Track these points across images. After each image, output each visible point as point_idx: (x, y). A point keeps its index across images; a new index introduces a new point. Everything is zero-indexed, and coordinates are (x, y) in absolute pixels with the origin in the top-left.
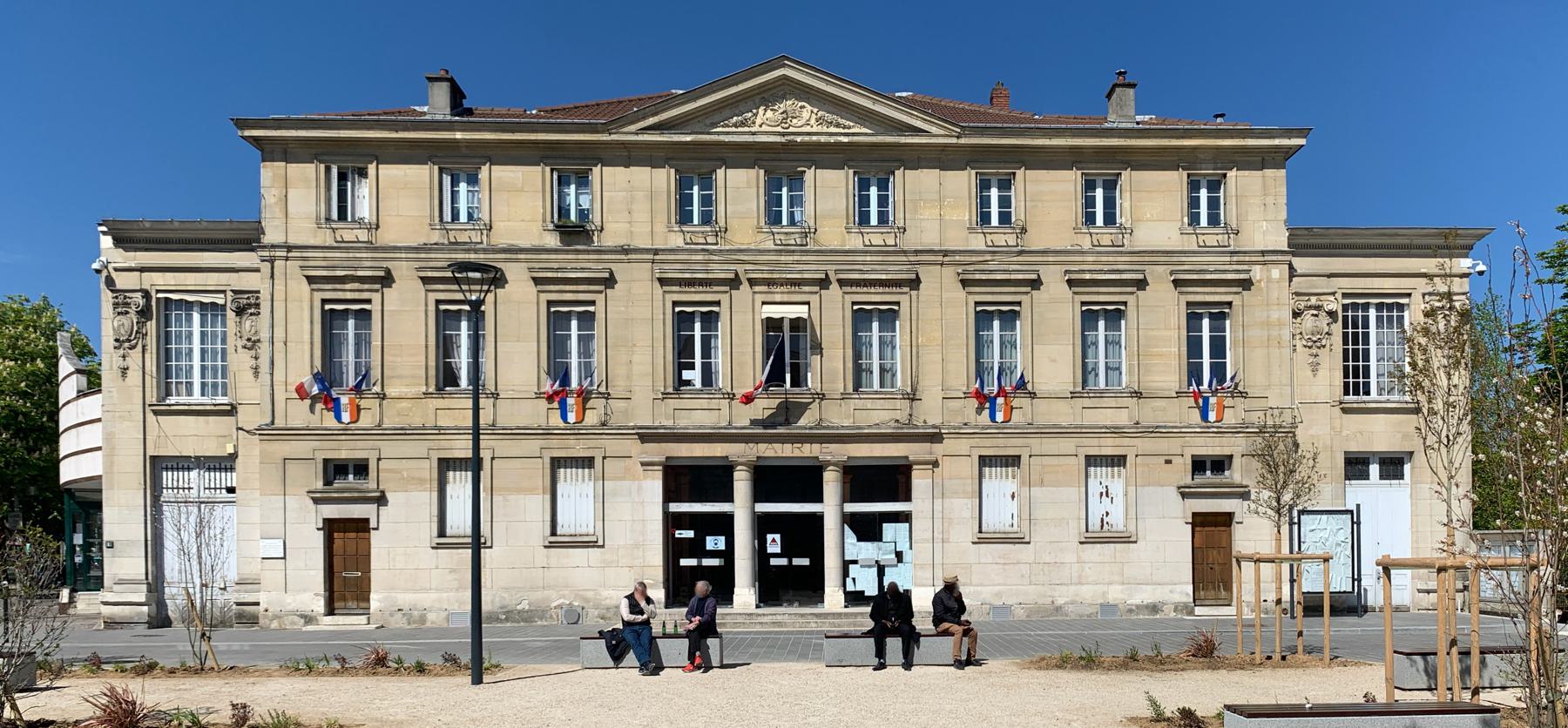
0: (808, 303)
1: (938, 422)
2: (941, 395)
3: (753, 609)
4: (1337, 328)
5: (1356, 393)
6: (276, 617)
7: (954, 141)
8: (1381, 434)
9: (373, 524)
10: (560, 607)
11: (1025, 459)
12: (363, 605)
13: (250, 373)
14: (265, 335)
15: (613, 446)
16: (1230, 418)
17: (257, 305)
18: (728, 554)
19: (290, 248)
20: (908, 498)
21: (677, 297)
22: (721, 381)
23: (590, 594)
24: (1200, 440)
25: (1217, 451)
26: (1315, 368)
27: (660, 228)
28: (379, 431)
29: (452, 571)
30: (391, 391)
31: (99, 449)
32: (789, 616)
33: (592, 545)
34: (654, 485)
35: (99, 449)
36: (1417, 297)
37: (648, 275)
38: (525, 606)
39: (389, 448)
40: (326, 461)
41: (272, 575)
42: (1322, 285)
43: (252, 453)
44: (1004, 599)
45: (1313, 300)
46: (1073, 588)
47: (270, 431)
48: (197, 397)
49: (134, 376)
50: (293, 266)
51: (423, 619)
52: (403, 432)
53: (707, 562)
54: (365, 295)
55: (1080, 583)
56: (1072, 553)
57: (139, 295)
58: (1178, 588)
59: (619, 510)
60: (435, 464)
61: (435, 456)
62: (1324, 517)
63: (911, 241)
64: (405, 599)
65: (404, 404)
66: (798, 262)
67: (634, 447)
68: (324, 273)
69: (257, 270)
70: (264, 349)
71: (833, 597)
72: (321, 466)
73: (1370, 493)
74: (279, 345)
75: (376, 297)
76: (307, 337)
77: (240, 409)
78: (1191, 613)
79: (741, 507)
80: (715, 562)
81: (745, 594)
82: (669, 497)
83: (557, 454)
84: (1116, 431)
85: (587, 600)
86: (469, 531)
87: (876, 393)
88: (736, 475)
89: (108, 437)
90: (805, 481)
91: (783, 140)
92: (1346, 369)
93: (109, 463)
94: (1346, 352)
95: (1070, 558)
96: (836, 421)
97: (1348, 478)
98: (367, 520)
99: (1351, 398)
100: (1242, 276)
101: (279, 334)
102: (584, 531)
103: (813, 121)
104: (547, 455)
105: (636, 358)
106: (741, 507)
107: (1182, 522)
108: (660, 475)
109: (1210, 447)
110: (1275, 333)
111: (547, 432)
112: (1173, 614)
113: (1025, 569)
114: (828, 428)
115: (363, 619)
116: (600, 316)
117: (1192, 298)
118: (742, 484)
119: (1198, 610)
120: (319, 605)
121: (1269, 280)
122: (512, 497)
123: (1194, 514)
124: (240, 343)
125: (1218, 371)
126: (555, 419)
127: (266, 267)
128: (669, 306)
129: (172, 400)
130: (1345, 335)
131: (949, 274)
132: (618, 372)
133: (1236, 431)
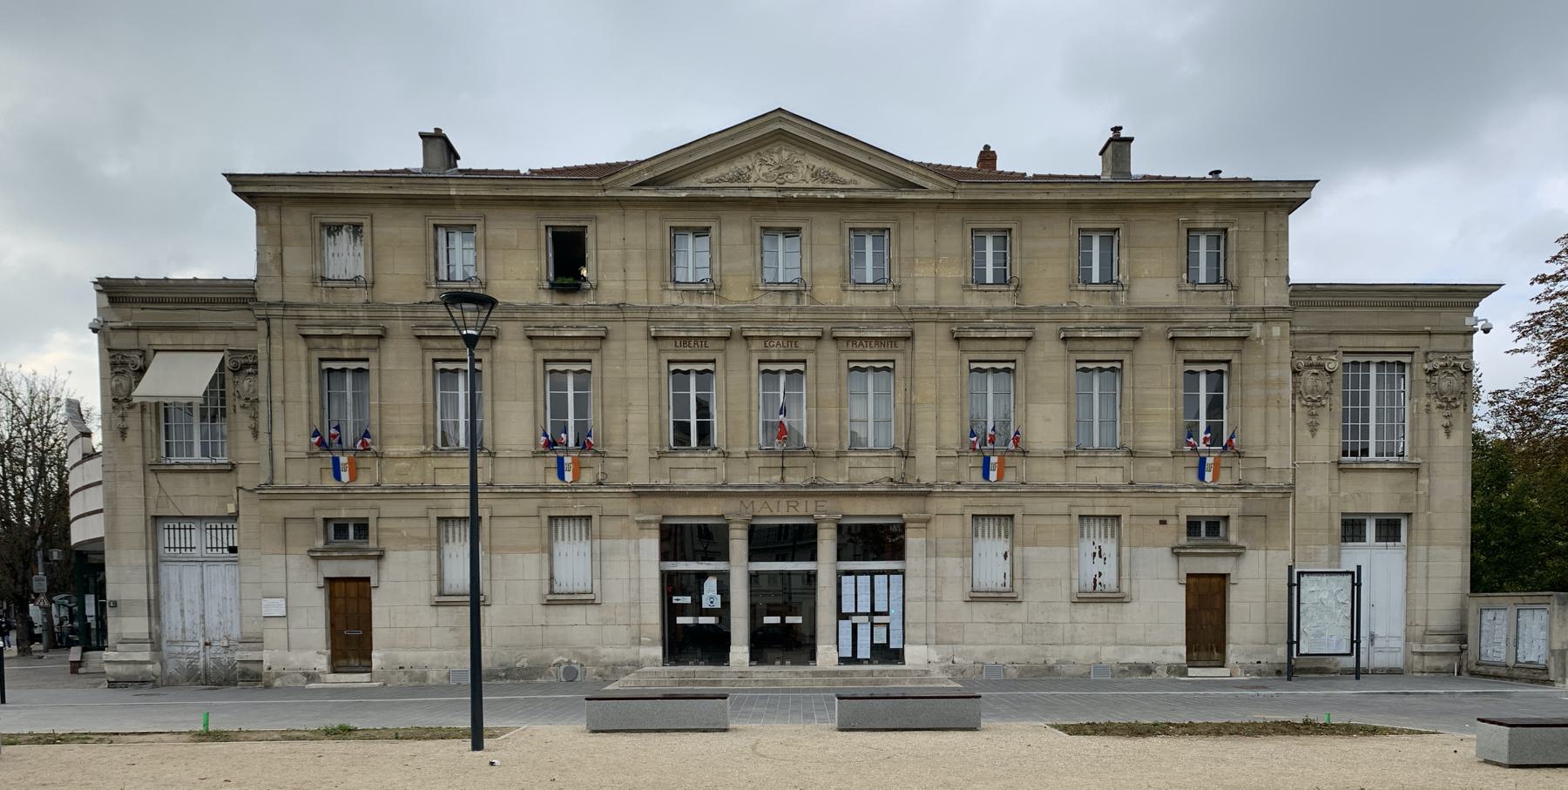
0: (804, 361)
1: (931, 480)
2: (934, 454)
3: (746, 667)
4: (1338, 387)
5: (1354, 454)
6: (279, 675)
7: (950, 197)
8: (1377, 496)
9: (373, 583)
10: (559, 664)
11: (1018, 519)
12: (365, 663)
15: (612, 505)
16: (1225, 478)
18: (724, 612)
19: (285, 305)
21: (672, 356)
22: (716, 438)
23: (588, 652)
24: (1196, 501)
25: (1213, 512)
27: (655, 286)
28: (379, 491)
29: (453, 629)
31: (100, 511)
32: (782, 673)
33: (592, 602)
35: (100, 511)
36: (1419, 356)
37: (643, 334)
38: (523, 663)
39: (389, 508)
40: (326, 520)
41: (274, 634)
42: (1322, 342)
43: (251, 511)
44: (996, 659)
45: (1314, 359)
46: (1065, 648)
47: (268, 492)
48: (197, 457)
49: (133, 437)
50: (290, 325)
51: (424, 677)
52: (401, 492)
53: (703, 620)
54: (363, 355)
55: (1073, 643)
56: (1063, 614)
57: (136, 355)
58: (1171, 649)
59: (618, 569)
60: (434, 523)
61: (434, 515)
62: (1325, 578)
63: (907, 298)
64: (406, 656)
65: (404, 464)
66: (794, 321)
67: (628, 506)
68: (321, 332)
69: (255, 329)
70: (263, 408)
71: (827, 655)
73: (1371, 556)
75: (373, 357)
76: (304, 396)
77: (240, 470)
78: (1185, 674)
79: (739, 566)
80: (711, 620)
81: (739, 652)
82: (664, 556)
83: (553, 513)
84: (1111, 490)
85: (585, 658)
86: (468, 589)
88: (733, 533)
89: (110, 498)
90: (800, 541)
91: (780, 195)
92: (1345, 428)
93: (111, 526)
94: (1345, 411)
95: (1063, 618)
96: (832, 479)
97: (1345, 539)
98: (368, 579)
99: (1349, 458)
100: (1242, 334)
102: (581, 589)
104: (545, 515)
105: (631, 418)
106: (739, 566)
107: (1175, 582)
108: (656, 534)
109: (1206, 508)
110: (1273, 392)
111: (544, 492)
112: (1165, 675)
113: (1018, 629)
114: (823, 486)
115: (365, 677)
116: (595, 376)
117: (1189, 356)
118: (739, 545)
119: (1192, 672)
120: (322, 663)
121: (1269, 338)
122: (511, 556)
123: (1189, 576)
124: (239, 403)
125: (1215, 431)
126: (553, 479)
127: (262, 326)
129: (174, 460)
130: (1345, 395)
131: (943, 330)
132: (616, 431)
133: (1231, 490)
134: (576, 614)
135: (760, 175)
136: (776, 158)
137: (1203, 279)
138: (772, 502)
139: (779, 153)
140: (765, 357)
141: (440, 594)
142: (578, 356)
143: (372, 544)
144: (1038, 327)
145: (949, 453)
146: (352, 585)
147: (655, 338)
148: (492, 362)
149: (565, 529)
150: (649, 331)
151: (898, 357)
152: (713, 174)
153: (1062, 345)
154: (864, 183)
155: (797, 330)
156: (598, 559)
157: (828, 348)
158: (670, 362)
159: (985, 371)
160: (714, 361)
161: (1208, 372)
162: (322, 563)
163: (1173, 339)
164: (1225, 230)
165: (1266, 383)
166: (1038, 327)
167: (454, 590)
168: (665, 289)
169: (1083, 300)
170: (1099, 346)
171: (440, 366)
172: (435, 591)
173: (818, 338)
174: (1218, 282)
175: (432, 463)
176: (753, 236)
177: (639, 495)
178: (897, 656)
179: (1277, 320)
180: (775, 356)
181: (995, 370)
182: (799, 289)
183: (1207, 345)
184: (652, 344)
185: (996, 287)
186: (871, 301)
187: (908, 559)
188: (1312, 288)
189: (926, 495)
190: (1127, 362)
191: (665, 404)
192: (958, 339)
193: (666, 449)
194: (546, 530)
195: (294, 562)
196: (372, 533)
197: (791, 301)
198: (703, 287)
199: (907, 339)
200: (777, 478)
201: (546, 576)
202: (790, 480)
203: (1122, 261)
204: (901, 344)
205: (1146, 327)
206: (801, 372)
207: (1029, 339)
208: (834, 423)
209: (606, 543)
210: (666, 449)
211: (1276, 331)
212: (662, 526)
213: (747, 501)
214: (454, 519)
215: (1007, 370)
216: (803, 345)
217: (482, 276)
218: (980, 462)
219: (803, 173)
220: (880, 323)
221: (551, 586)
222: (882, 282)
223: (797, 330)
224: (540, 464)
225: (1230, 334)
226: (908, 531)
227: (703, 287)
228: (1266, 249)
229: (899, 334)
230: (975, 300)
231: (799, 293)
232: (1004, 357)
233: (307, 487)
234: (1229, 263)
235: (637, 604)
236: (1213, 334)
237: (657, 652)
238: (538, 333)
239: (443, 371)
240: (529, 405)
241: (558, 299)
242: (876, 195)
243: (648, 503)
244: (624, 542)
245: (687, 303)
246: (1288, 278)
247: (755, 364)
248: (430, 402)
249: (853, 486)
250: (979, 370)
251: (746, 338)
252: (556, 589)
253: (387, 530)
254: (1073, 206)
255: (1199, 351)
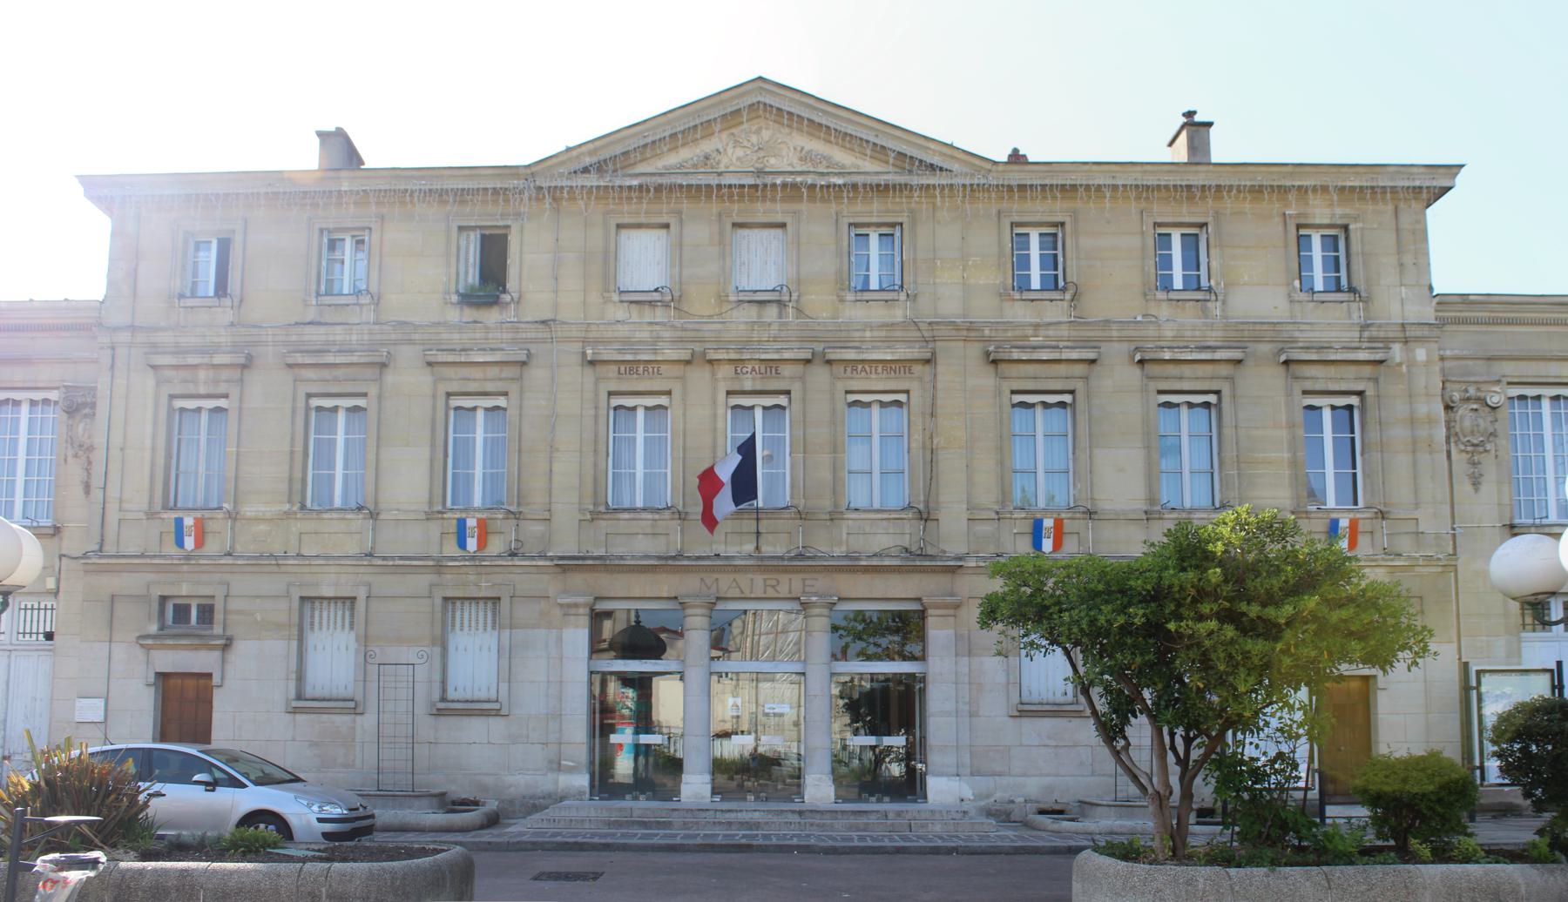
0: (788, 393)
1: (963, 550)
2: (965, 516)
9: (216, 679)
13: (79, 490)
14: (100, 440)
17: (93, 405)
20: (922, 658)
21: (613, 388)
23: (489, 780)
26: (1476, 483)
29: (313, 744)
30: (248, 510)
33: (497, 713)
34: (578, 637)
37: (577, 359)
45: (1472, 391)
61: (296, 594)
65: (263, 527)
67: (550, 584)
72: (155, 606)
74: (115, 453)
83: (450, 594)
87: (878, 511)
98: (209, 676)
100: (1378, 357)
101: (116, 440)
102: (483, 695)
103: (795, 161)
105: (557, 467)
110: (1422, 433)
111: (439, 567)
117: (1309, 386)
121: (1412, 363)
126: (451, 548)
128: (604, 396)
134: (475, 728)
135: (733, 156)
136: (754, 139)
137: (1319, 286)
138: (744, 580)
139: (758, 131)
140: (737, 388)
141: (299, 697)
142: (489, 387)
143: (217, 629)
144: (1104, 347)
145: (984, 515)
146: (191, 683)
147: (592, 363)
148: (380, 397)
149: (467, 613)
150: (584, 354)
151: (915, 388)
152: (672, 159)
153: (1137, 371)
154: (868, 165)
155: (778, 351)
156: (508, 657)
157: (820, 376)
158: (610, 394)
159: (1032, 406)
160: (669, 393)
161: (1333, 408)
162: (153, 653)
163: (1286, 363)
164: (1346, 228)
165: (1412, 421)
166: (1104, 347)
167: (318, 693)
168: (607, 301)
169: (1164, 312)
170: (1186, 370)
171: (315, 402)
172: (293, 694)
173: (808, 361)
174: (1339, 290)
175: (296, 527)
176: (721, 233)
177: (564, 569)
178: (911, 786)
179: (1420, 340)
180: (748, 386)
181: (1046, 405)
182: (778, 300)
183: (1332, 371)
184: (589, 371)
185: (1047, 295)
186: (878, 314)
187: (930, 659)
188: (1464, 299)
189: (953, 570)
190: (1226, 393)
191: (602, 448)
192: (995, 362)
193: (602, 508)
194: (438, 616)
195: (120, 651)
196: (218, 616)
197: (771, 312)
198: (656, 296)
199: (928, 361)
200: (749, 547)
201: (437, 677)
202: (767, 550)
203: (1214, 264)
204: (917, 369)
205: (1252, 347)
206: (783, 408)
207: (1093, 361)
208: (825, 474)
209: (519, 634)
210: (602, 508)
211: (1421, 354)
212: (592, 610)
213: (709, 578)
214: (322, 598)
215: (1062, 405)
216: (787, 370)
217: (374, 289)
218: (1027, 527)
219: (789, 153)
220: (889, 342)
221: (444, 690)
222: (896, 289)
223: (778, 351)
224: (435, 529)
225: (1362, 356)
226: (931, 621)
227: (656, 296)
228: (1400, 250)
229: (917, 356)
230: (1020, 313)
231: (780, 304)
232: (1059, 387)
233: (142, 556)
234: (1354, 267)
235: (557, 716)
236: (1339, 357)
237: (582, 781)
238: (440, 359)
239: (319, 409)
240: (425, 452)
241: (470, 314)
242: (882, 179)
243: (577, 580)
244: (541, 633)
245: (635, 318)
246: (1431, 288)
247: (722, 396)
248: (299, 448)
249: (852, 558)
250: (1023, 405)
251: (710, 362)
252: (451, 694)
253: (238, 612)
254: (1144, 191)
255: (1320, 377)
